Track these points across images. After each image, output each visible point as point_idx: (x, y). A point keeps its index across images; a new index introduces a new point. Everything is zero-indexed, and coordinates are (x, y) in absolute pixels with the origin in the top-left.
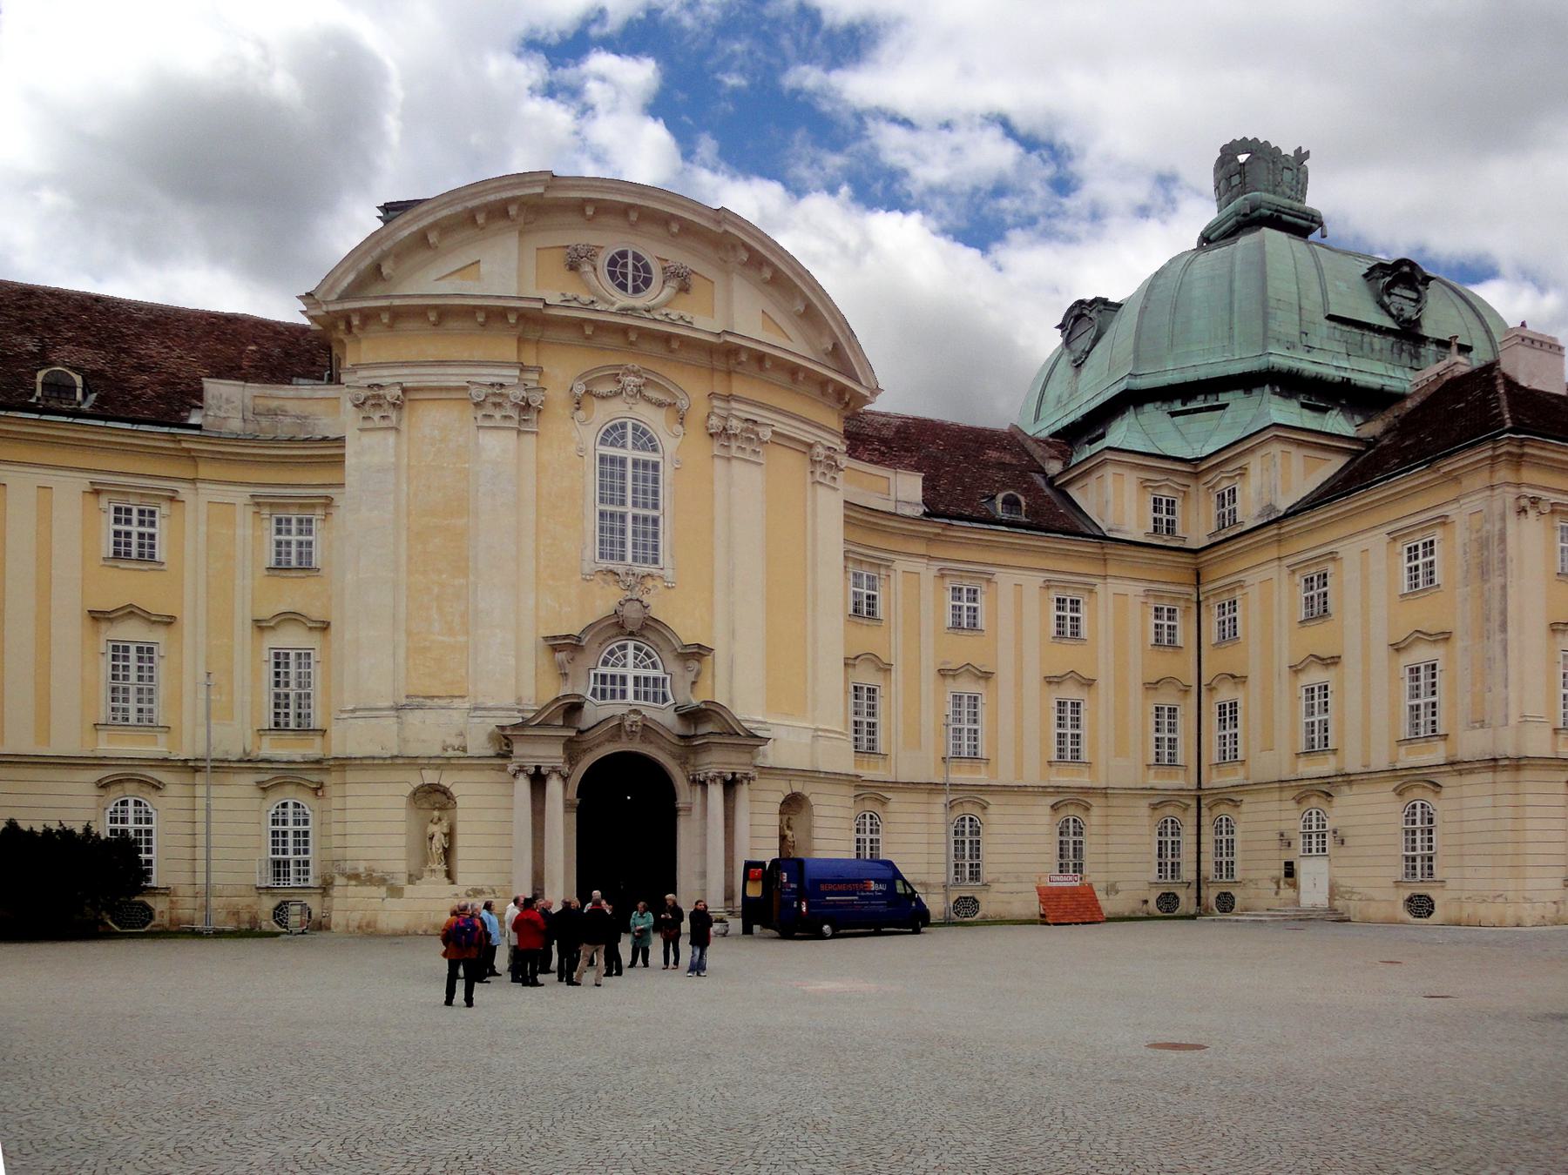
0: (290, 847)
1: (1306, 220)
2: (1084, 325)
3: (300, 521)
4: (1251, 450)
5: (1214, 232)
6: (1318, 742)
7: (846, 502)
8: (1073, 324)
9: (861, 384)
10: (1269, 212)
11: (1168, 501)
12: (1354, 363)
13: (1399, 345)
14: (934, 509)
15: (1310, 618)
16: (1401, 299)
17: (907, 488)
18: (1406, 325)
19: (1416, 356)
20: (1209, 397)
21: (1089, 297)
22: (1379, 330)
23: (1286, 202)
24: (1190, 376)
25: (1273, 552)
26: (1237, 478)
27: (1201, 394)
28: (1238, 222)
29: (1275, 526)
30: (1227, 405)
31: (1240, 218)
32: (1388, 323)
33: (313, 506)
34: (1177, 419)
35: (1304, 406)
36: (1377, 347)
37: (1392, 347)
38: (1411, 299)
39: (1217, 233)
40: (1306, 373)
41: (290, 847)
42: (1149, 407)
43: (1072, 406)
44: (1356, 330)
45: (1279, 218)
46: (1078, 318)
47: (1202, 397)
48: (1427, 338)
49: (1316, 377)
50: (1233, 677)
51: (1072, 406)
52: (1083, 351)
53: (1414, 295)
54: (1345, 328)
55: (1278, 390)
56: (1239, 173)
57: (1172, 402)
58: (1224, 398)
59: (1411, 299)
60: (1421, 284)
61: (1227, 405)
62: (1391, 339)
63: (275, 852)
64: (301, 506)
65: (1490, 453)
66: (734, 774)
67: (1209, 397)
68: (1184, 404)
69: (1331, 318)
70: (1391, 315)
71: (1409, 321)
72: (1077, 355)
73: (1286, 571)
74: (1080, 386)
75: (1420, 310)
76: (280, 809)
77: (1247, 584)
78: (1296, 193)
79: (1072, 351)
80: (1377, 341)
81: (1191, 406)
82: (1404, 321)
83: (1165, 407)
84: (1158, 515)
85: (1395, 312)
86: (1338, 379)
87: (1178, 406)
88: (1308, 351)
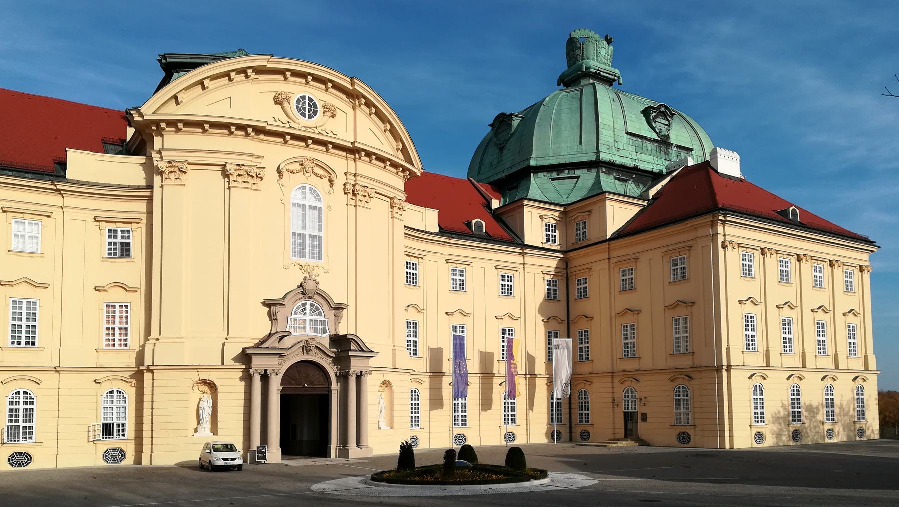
0: (21, 418)
1: (612, 75)
5: (566, 77)
6: (629, 353)
7: (405, 226)
8: (499, 125)
9: (414, 166)
10: (594, 71)
11: (552, 225)
14: (444, 231)
15: (624, 290)
17: (428, 219)
18: (663, 138)
19: (667, 153)
20: (570, 171)
23: (603, 66)
24: (562, 161)
30: (580, 176)
32: (655, 136)
35: (616, 178)
36: (649, 148)
37: (656, 149)
38: (665, 125)
40: (617, 162)
41: (21, 418)
42: (541, 174)
44: (640, 140)
45: (599, 74)
46: (502, 122)
47: (566, 171)
48: (672, 144)
49: (622, 164)
50: (586, 317)
53: (667, 123)
58: (578, 172)
59: (665, 125)
60: (670, 117)
61: (580, 176)
63: (11, 421)
66: (361, 372)
67: (570, 171)
68: (558, 175)
69: (628, 133)
70: (656, 132)
71: (664, 136)
75: (669, 130)
76: (15, 395)
77: (593, 270)
80: (650, 146)
82: (661, 136)
83: (549, 175)
84: (548, 233)
85: (658, 131)
86: (632, 166)
87: (555, 175)
88: (618, 151)
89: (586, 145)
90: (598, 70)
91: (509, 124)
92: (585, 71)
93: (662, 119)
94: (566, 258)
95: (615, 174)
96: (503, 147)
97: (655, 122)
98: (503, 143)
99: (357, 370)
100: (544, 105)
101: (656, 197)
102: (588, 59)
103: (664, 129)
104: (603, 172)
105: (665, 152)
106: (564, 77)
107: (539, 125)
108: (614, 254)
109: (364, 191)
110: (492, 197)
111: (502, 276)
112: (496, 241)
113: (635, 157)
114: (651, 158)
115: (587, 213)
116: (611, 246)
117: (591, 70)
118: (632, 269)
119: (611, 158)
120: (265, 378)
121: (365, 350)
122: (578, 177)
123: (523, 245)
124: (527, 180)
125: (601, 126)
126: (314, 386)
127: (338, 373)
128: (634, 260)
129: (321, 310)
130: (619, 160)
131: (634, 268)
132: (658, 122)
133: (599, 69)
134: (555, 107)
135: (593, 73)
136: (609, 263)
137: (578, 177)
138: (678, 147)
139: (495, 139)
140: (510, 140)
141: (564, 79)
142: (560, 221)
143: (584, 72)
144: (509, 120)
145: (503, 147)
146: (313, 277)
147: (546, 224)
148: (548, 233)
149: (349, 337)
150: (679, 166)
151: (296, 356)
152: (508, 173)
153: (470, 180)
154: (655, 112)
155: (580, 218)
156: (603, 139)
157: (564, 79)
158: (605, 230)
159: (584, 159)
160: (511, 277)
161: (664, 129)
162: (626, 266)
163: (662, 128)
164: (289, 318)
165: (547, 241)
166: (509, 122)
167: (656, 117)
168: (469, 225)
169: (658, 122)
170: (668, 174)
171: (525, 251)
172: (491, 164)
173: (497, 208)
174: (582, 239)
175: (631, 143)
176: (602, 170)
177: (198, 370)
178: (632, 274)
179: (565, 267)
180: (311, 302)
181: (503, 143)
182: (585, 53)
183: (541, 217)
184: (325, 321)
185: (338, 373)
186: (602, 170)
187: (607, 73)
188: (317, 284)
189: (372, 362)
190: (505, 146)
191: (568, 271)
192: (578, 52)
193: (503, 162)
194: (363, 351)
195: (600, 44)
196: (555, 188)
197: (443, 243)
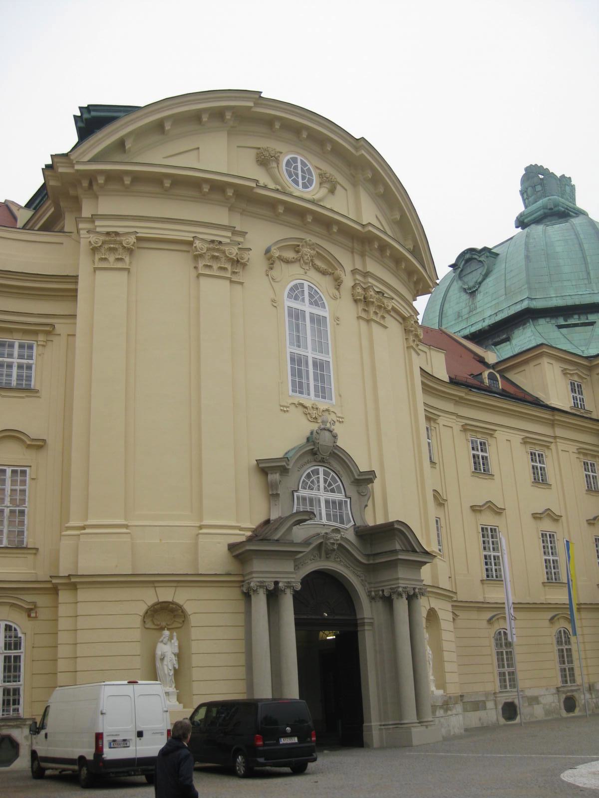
2: (473, 265)
3: (21, 346)
5: (527, 218)
10: (563, 209)
21: (479, 247)
24: (569, 302)
27: (576, 314)
28: (545, 213)
30: (595, 322)
31: (546, 211)
33: (36, 333)
39: (529, 219)
42: (542, 321)
43: (473, 320)
46: (468, 261)
47: (576, 317)
51: (473, 320)
52: (476, 282)
56: (541, 184)
57: (557, 318)
58: (592, 318)
61: (595, 322)
64: (25, 332)
67: (582, 317)
72: (471, 284)
74: (478, 305)
79: (464, 283)
83: (553, 321)
87: (561, 321)
89: (596, 283)
90: (567, 209)
96: (474, 291)
98: (474, 287)
99: (409, 586)
109: (379, 300)
120: (273, 596)
121: (418, 550)
124: (524, 329)
126: (336, 617)
127: (373, 593)
129: (340, 482)
133: (568, 208)
140: (485, 282)
144: (480, 257)
145: (475, 291)
146: (328, 425)
147: (571, 383)
149: (396, 526)
151: (310, 562)
164: (295, 494)
171: (557, 418)
177: (156, 585)
180: (326, 469)
183: (565, 373)
184: (346, 502)
185: (373, 593)
188: (335, 437)
189: (426, 573)
190: (477, 289)
192: (539, 188)
193: (478, 310)
194: (414, 551)
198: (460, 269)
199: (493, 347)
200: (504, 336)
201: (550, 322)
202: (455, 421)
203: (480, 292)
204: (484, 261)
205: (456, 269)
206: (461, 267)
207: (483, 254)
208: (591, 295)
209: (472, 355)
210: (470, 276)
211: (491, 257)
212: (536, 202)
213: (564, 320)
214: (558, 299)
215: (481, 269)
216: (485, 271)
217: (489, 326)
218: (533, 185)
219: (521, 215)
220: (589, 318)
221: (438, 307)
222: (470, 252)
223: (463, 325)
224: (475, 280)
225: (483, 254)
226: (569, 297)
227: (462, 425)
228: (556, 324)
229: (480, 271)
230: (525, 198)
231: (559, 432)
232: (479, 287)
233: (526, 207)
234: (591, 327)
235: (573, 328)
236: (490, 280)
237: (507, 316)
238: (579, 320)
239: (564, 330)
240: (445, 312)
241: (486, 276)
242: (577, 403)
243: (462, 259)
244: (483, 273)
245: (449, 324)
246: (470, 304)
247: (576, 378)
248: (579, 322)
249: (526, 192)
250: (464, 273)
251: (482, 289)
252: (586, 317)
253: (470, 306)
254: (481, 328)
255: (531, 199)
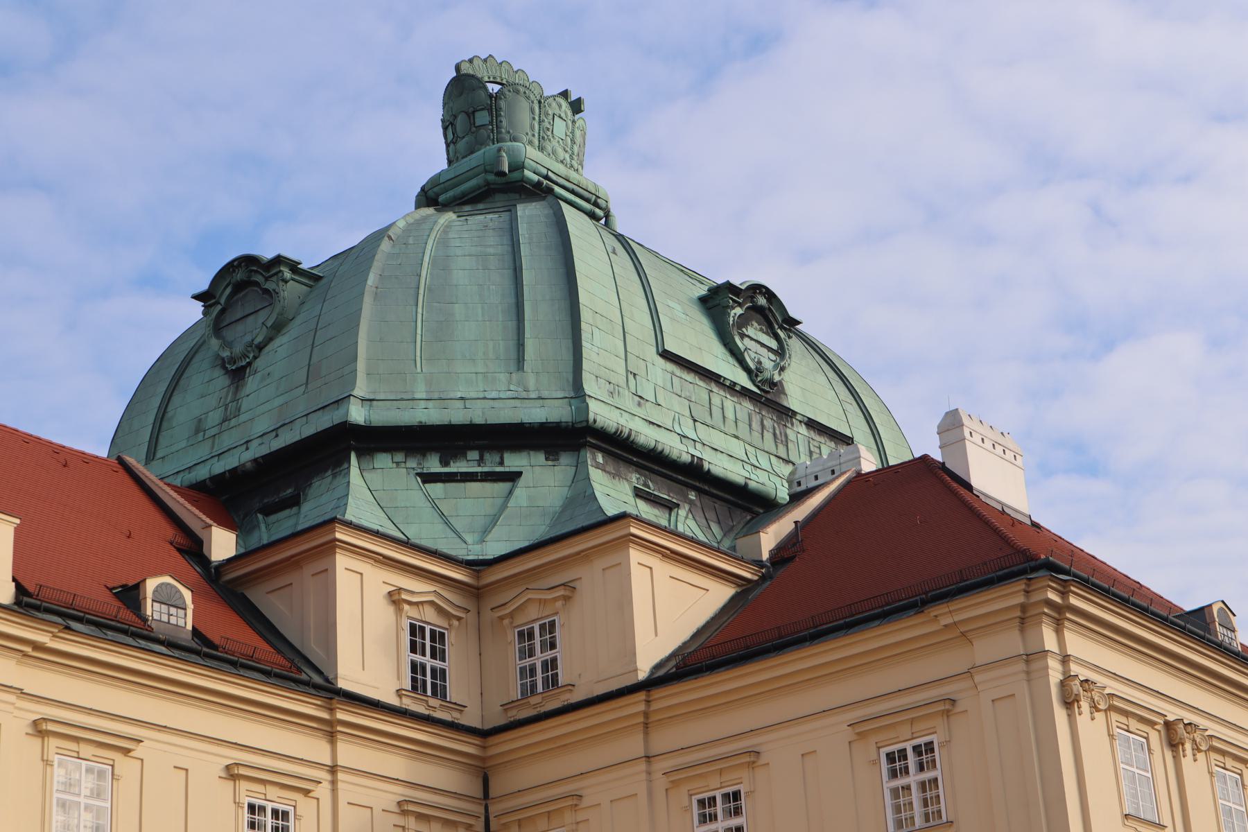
1: (588, 200)
4: (583, 557)
5: (446, 191)
10: (535, 178)
11: (433, 632)
12: (704, 433)
13: (758, 417)
16: (756, 341)
20: (487, 456)
21: (268, 254)
22: (731, 388)
23: (560, 169)
24: (457, 415)
25: (634, 745)
26: (559, 604)
27: (472, 448)
29: (642, 696)
30: (519, 474)
31: (491, 177)
32: (742, 379)
34: (431, 487)
35: (638, 493)
36: (730, 414)
38: (770, 349)
39: (451, 194)
40: (641, 440)
42: (383, 460)
43: (227, 440)
44: (701, 383)
46: (239, 287)
47: (473, 455)
48: (795, 413)
49: (654, 450)
51: (227, 440)
52: (250, 344)
53: (774, 344)
54: (690, 377)
55: (600, 458)
57: (424, 455)
58: (513, 462)
59: (770, 349)
60: (781, 327)
61: (519, 474)
62: (747, 405)
65: (1020, 599)
67: (487, 456)
68: (445, 463)
69: (667, 355)
72: (238, 349)
73: (661, 783)
74: (245, 404)
75: (782, 369)
77: (586, 802)
78: (572, 158)
79: (227, 344)
80: (730, 403)
81: (455, 467)
82: (764, 382)
83: (412, 463)
84: (418, 658)
85: (752, 365)
86: (686, 458)
87: (433, 465)
88: (639, 404)
90: (547, 177)
91: (266, 291)
92: (507, 171)
93: (761, 330)
94: (483, 759)
95: (635, 478)
96: (243, 368)
97: (743, 336)
100: (390, 238)
101: (784, 554)
102: (514, 139)
103: (768, 361)
104: (597, 466)
105: (775, 434)
106: (435, 189)
107: (376, 296)
108: (664, 739)
110: (211, 522)
111: (252, 808)
112: (233, 664)
113: (692, 435)
114: (737, 448)
115: (560, 592)
116: (655, 706)
117: (528, 173)
118: (736, 796)
119: (622, 421)
122: (513, 477)
123: (331, 692)
124: (334, 476)
125: (585, 315)
128: (746, 759)
130: (647, 436)
131: (743, 789)
132: (752, 339)
133: (550, 174)
134: (429, 247)
135: (530, 181)
136: (649, 773)
137: (513, 477)
138: (812, 424)
139: (215, 343)
141: (438, 195)
142: (459, 619)
143: (502, 174)
144: (267, 279)
145: (243, 368)
147: (412, 627)
148: (418, 658)
150: (833, 472)
152: (264, 451)
153: (121, 461)
154: (740, 305)
155: (533, 612)
156: (594, 357)
157: (438, 195)
158: (630, 653)
159: (536, 414)
160: (285, 815)
161: (768, 361)
162: (714, 782)
163: (762, 360)
165: (414, 688)
166: (269, 286)
167: (743, 321)
168: (130, 595)
169: (752, 339)
170: (797, 498)
171: (341, 715)
172: (199, 427)
173: (230, 561)
174: (540, 688)
175: (677, 389)
176: (594, 459)
178: (737, 812)
179: (480, 794)
181: (245, 356)
182: (504, 123)
183: (395, 598)
186: (594, 459)
187: (573, 192)
190: (249, 364)
191: (491, 809)
192: (482, 118)
193: (243, 418)
195: (550, 105)
196: (435, 507)
197: (28, 649)
198: (219, 307)
199: (260, 517)
200: (290, 491)
201: (403, 465)
202: (9, 708)
203: (256, 372)
204: (274, 290)
205: (211, 306)
206: (223, 301)
207: (276, 274)
208: (517, 403)
209: (169, 531)
210: (240, 328)
211: (293, 279)
212: (472, 153)
213: (441, 462)
214: (430, 404)
215: (266, 311)
216: (274, 316)
217: (255, 460)
218: (471, 110)
219: (435, 182)
220: (506, 462)
221: (156, 402)
222: (247, 266)
223: (203, 451)
224: (248, 338)
225: (276, 274)
226: (460, 404)
227: (35, 722)
228: (419, 471)
229: (262, 316)
230: (449, 141)
231: (350, 753)
232: (255, 358)
233: (450, 162)
234: (507, 485)
235: (462, 484)
236: (282, 345)
237: (298, 438)
238: (479, 466)
239: (436, 489)
240: (169, 415)
241: (278, 328)
242: (424, 682)
243: (228, 281)
244: (269, 324)
245: (174, 449)
246: (229, 399)
247: (430, 615)
248: (479, 469)
249: (452, 124)
250: (229, 318)
251: (259, 363)
252: (498, 459)
253: (226, 406)
254: (235, 464)
255: (461, 145)
